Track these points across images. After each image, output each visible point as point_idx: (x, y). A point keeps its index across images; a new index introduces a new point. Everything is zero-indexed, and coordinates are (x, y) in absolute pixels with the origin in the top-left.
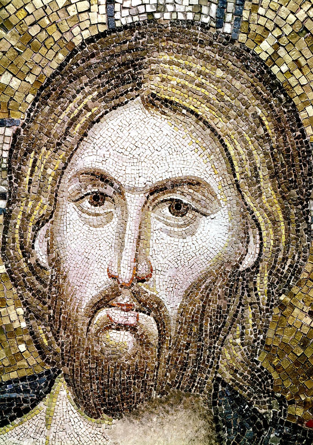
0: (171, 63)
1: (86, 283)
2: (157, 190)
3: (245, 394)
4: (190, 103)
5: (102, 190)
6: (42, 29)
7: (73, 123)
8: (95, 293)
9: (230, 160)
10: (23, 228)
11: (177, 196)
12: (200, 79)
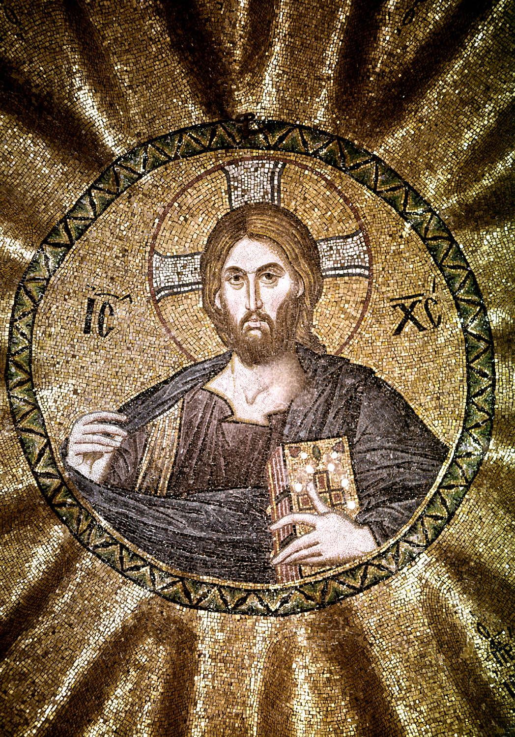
0: (257, 219)
1: (238, 313)
2: (259, 270)
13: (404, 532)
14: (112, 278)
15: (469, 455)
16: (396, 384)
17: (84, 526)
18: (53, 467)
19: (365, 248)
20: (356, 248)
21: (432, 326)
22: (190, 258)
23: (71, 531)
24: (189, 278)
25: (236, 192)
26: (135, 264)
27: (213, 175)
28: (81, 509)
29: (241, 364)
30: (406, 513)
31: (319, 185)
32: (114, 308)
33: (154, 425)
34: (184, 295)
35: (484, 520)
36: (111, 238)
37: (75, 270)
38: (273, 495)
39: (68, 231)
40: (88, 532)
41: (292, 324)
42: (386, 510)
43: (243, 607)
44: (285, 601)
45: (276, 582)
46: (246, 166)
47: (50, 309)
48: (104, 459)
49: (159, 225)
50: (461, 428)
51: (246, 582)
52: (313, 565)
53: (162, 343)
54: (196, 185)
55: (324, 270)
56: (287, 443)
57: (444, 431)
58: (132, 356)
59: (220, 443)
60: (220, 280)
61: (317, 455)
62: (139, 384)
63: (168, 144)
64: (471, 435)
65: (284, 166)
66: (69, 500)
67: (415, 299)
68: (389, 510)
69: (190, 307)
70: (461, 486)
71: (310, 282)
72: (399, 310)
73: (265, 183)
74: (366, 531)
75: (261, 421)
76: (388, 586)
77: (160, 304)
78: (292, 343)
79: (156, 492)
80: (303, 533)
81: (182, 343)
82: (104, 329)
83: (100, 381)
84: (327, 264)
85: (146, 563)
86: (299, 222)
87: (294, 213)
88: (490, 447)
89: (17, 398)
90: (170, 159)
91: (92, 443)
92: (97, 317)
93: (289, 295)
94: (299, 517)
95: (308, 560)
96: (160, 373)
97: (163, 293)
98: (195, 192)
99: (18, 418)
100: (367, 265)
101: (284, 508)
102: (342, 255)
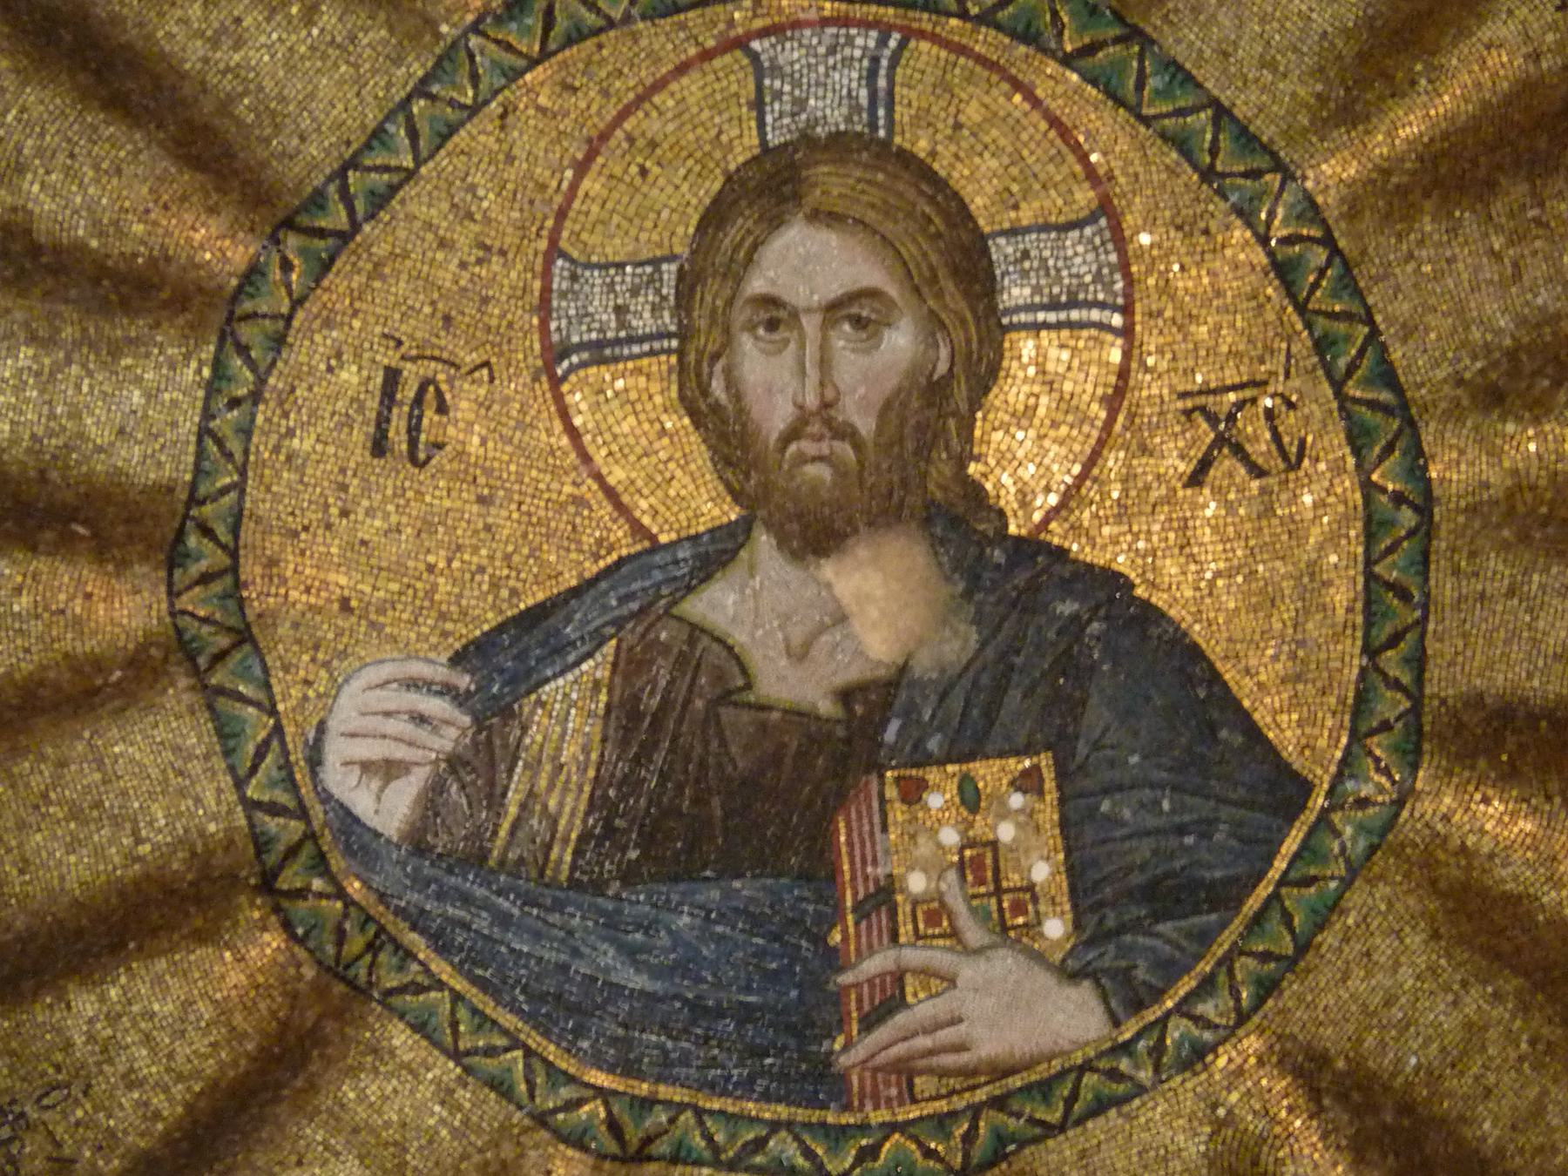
1: (775, 416)
4: (856, 211)
7: (736, 249)
8: (782, 426)
9: (905, 263)
10: (699, 362)
11: (854, 310)
13: (1182, 993)
14: (447, 319)
15: (1363, 803)
17: (356, 944)
19: (1113, 258)
20: (1090, 257)
21: (1282, 466)
22: (649, 269)
23: (320, 963)
24: (643, 322)
25: (777, 106)
27: (717, 63)
28: (346, 906)
29: (775, 553)
30: (1192, 948)
31: (995, 92)
32: (448, 397)
34: (630, 365)
35: (1375, 957)
39: (347, 198)
40: (368, 958)
41: (916, 453)
42: (1141, 939)
43: (759, 1159)
45: (847, 1108)
47: (293, 390)
48: (412, 778)
49: (574, 187)
52: (943, 1073)
53: (568, 489)
54: (674, 86)
57: (1303, 741)
58: (490, 520)
59: (711, 760)
60: (727, 331)
61: (970, 798)
62: (505, 593)
64: (1370, 753)
65: (902, 45)
66: (317, 884)
69: (645, 397)
71: (968, 342)
73: (854, 85)
74: (1084, 993)
76: (1130, 1118)
77: (565, 388)
78: (914, 500)
79: (542, 874)
80: (922, 995)
81: (620, 489)
84: (1016, 293)
85: (515, 1044)
86: (940, 184)
88: (1419, 785)
89: (193, 615)
90: (611, 24)
91: (384, 737)
93: (913, 372)
94: (913, 956)
95: (935, 1061)
97: (575, 359)
98: (671, 103)
99: (202, 661)
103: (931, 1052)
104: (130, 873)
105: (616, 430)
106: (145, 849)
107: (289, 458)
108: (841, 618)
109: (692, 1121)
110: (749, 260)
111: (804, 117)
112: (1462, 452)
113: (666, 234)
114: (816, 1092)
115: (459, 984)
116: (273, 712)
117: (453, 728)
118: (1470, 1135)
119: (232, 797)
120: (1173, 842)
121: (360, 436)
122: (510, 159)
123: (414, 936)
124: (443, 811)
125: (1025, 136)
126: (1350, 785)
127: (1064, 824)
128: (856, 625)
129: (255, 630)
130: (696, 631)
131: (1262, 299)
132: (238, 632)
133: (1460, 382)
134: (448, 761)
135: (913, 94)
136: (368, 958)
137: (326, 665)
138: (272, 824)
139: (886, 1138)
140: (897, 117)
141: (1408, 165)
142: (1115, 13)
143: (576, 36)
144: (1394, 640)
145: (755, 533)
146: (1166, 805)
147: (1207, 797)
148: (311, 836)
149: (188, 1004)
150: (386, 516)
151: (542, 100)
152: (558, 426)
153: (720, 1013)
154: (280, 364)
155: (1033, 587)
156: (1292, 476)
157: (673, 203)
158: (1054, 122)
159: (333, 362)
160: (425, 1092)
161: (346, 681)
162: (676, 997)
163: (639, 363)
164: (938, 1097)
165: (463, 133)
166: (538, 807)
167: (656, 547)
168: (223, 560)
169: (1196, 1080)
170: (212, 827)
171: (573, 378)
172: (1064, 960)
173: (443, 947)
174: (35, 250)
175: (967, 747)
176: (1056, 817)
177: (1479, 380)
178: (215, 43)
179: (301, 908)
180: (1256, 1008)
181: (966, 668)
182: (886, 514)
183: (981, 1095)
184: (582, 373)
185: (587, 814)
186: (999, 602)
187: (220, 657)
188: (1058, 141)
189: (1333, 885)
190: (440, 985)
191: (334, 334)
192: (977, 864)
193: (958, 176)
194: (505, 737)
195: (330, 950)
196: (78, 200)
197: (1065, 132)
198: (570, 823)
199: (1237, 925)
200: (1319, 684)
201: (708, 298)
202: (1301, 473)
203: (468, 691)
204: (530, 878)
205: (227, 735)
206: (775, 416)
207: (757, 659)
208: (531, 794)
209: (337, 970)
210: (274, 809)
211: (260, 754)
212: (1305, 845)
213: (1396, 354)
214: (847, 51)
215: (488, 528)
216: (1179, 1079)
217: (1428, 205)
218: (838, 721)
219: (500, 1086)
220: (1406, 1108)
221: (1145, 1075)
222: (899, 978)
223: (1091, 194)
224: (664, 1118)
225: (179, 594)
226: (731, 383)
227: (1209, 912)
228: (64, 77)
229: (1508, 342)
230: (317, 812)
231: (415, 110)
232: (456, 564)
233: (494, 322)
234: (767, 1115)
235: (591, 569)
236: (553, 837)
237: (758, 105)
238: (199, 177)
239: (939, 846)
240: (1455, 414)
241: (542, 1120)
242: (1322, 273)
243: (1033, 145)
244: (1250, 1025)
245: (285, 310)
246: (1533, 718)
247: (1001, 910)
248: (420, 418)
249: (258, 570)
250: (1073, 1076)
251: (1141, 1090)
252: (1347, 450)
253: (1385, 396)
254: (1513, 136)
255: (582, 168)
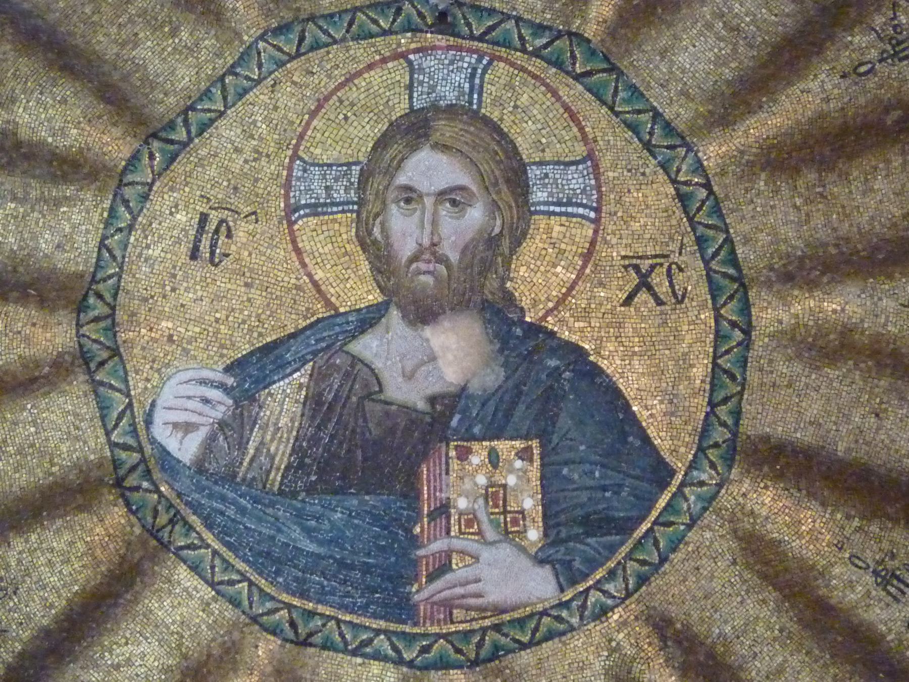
1: (406, 249)
2: (442, 195)
3: (500, 306)
5: (410, 195)
6: (375, 114)
7: (392, 160)
12: (462, 133)
15: (702, 484)
16: (617, 375)
17: (163, 519)
18: (132, 437)
19: (593, 182)
21: (673, 301)
22: (345, 168)
23: (143, 526)
24: (339, 195)
26: (268, 171)
27: (390, 65)
28: (159, 497)
30: (605, 553)
31: (537, 91)
32: (233, 229)
33: (270, 394)
34: (331, 217)
35: (701, 571)
36: (242, 137)
37: (188, 174)
38: (426, 509)
40: (169, 528)
41: (480, 273)
42: (578, 545)
43: (368, 650)
44: (425, 650)
45: (416, 624)
46: (438, 57)
47: (151, 224)
48: (200, 433)
49: (308, 124)
50: (695, 446)
51: (375, 618)
52: (468, 609)
53: (293, 281)
54: (366, 75)
55: (534, 204)
56: (454, 440)
57: (673, 448)
58: (251, 296)
59: (358, 430)
60: (384, 203)
62: (255, 335)
63: (335, 22)
65: (490, 63)
66: (145, 484)
67: (655, 261)
68: (582, 547)
69: (337, 234)
70: (683, 524)
71: (512, 218)
72: (632, 272)
73: (462, 81)
74: (546, 572)
75: (421, 405)
76: (565, 644)
77: (296, 227)
78: (477, 298)
79: (264, 487)
80: (460, 565)
81: (320, 282)
82: (217, 255)
83: (203, 326)
84: (539, 195)
85: (244, 578)
87: (499, 123)
88: (732, 477)
89: (88, 337)
90: (335, 42)
91: (186, 410)
92: (209, 239)
93: (480, 231)
94: (457, 544)
96: (286, 323)
97: (302, 212)
98: (364, 84)
99: (93, 366)
100: (595, 205)
101: (438, 529)
102: (560, 186)
103: (463, 596)
104: (47, 482)
105: (321, 250)
106: (55, 469)
107: (146, 260)
108: (433, 358)
109: (335, 626)
110: (399, 166)
111: (434, 95)
112: (769, 303)
113: (356, 151)
114: (400, 614)
115: (216, 545)
116: (128, 395)
117: (223, 405)
118: (744, 677)
119: (103, 439)
120: (599, 495)
121: (184, 249)
122: (276, 108)
123: (194, 518)
124: (214, 450)
125: (551, 115)
126: (695, 473)
127: (542, 478)
128: (440, 362)
129: (122, 350)
130: (356, 360)
131: (670, 212)
132: (113, 350)
133: (771, 269)
134: (219, 424)
135: (493, 89)
136: (169, 528)
137: (158, 371)
138: (123, 455)
139: (436, 641)
140: (484, 99)
141: (754, 150)
142: (604, 55)
143: (316, 46)
144: (726, 400)
145: (391, 310)
146: (597, 474)
147: (619, 472)
148: (143, 460)
149: (71, 544)
150: (196, 291)
151: (295, 78)
152: (290, 246)
153: (352, 567)
154: (145, 211)
155: (536, 350)
156: (678, 306)
157: (360, 135)
158: (567, 109)
159: (173, 210)
160: (194, 603)
161: (168, 379)
162: (331, 557)
163: (335, 216)
164: (467, 621)
165: (251, 93)
166: (265, 450)
167: (338, 315)
168: (106, 310)
169: (602, 626)
170: (92, 457)
171: (300, 222)
172: (537, 553)
173: (210, 527)
174: (18, 145)
175: (496, 432)
176: (539, 475)
177: (782, 269)
178: (123, 45)
179: (135, 496)
180: (636, 591)
181: (497, 391)
182: (461, 304)
183: (487, 623)
184: (305, 220)
185: (291, 455)
186: (518, 356)
187: (102, 364)
188: (569, 119)
189: (682, 527)
190: (208, 546)
191: (175, 195)
192: (495, 495)
193: (513, 133)
194: (250, 412)
195: (150, 519)
196: (43, 116)
197: (573, 116)
198: (282, 459)
199: (629, 544)
200: (683, 418)
201: (376, 185)
202: (683, 306)
203: (232, 386)
204: (259, 493)
205: (104, 408)
206: (406, 249)
207: (386, 376)
208: (262, 443)
209: (153, 532)
210: (126, 447)
211: (120, 418)
212: (669, 505)
213: (739, 251)
214: (460, 64)
215: (249, 300)
216: (593, 624)
217: (763, 176)
218: (427, 413)
219: (235, 602)
220: (711, 655)
221: (575, 621)
222: (448, 554)
223: (584, 148)
224: (319, 623)
225: (82, 326)
226: (383, 230)
227: (617, 534)
228: (40, 54)
229: (799, 253)
230: (148, 449)
231: (227, 81)
232: (231, 319)
233: (261, 191)
234: (374, 626)
235: (303, 324)
236: (271, 467)
237: (410, 87)
238: (109, 107)
239: (476, 484)
240: (769, 284)
241: (255, 619)
242: (703, 202)
243: (555, 120)
244: (633, 599)
245: (149, 181)
246: (795, 452)
247: (506, 523)
248: (217, 239)
249: (125, 317)
250: (537, 617)
251: (572, 629)
252: (709, 297)
253: (731, 271)
254: (811, 142)
255: (313, 114)
